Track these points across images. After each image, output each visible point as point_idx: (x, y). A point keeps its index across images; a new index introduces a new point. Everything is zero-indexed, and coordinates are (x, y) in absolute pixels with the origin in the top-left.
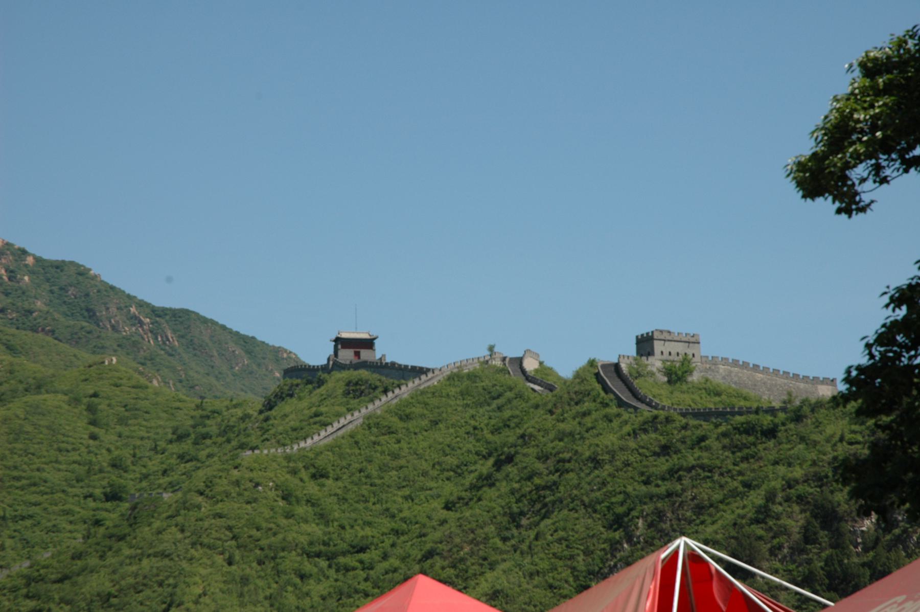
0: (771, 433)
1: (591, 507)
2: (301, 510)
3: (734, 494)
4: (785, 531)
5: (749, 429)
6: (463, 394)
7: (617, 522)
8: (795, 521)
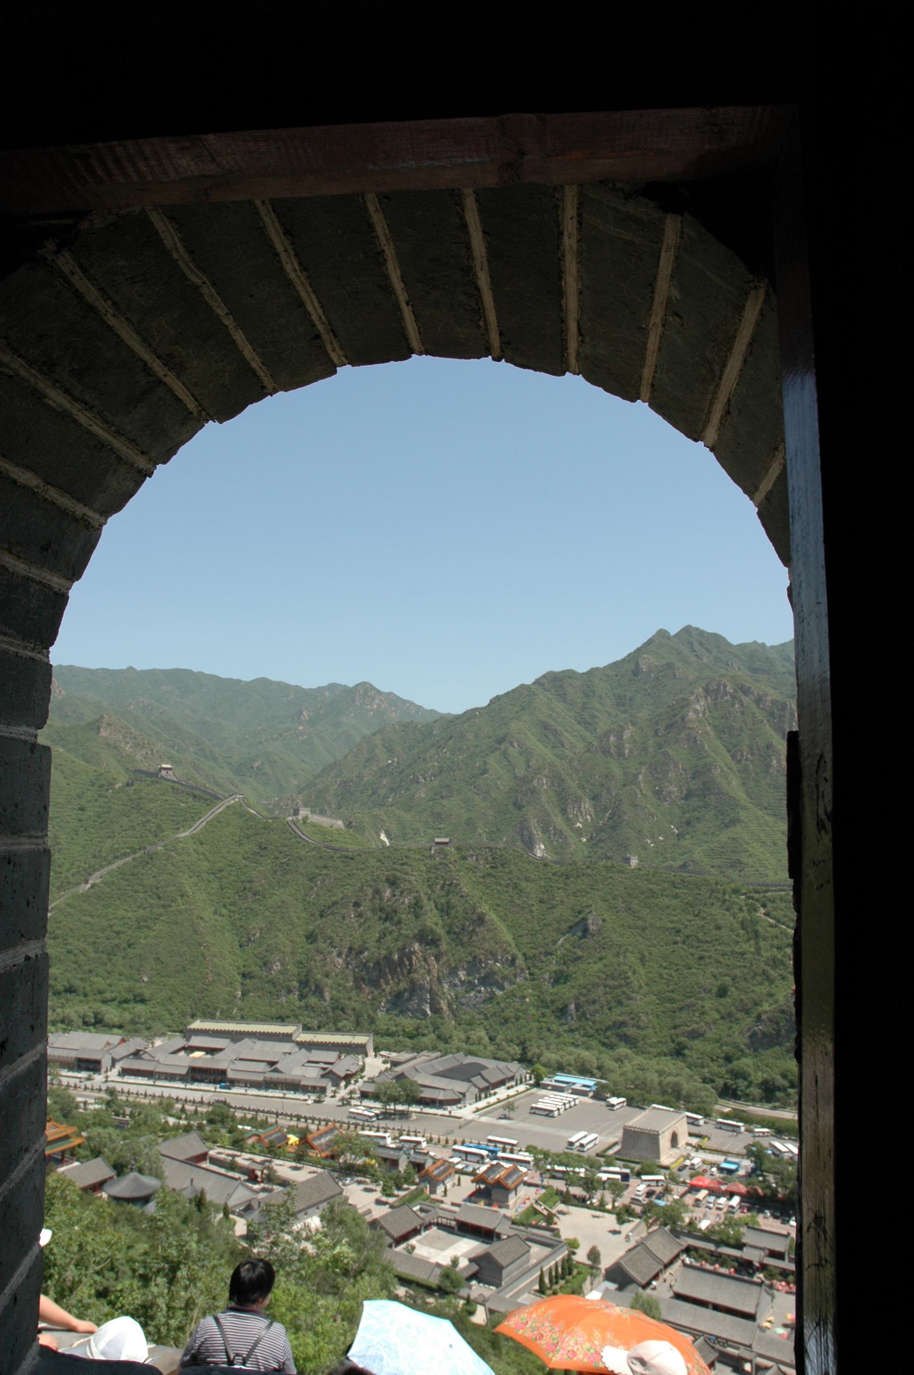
0: (353, 859)
1: (302, 874)
2: (202, 857)
3: (345, 877)
4: (367, 895)
5: (346, 857)
6: (234, 813)
7: (311, 880)
8: (370, 891)
